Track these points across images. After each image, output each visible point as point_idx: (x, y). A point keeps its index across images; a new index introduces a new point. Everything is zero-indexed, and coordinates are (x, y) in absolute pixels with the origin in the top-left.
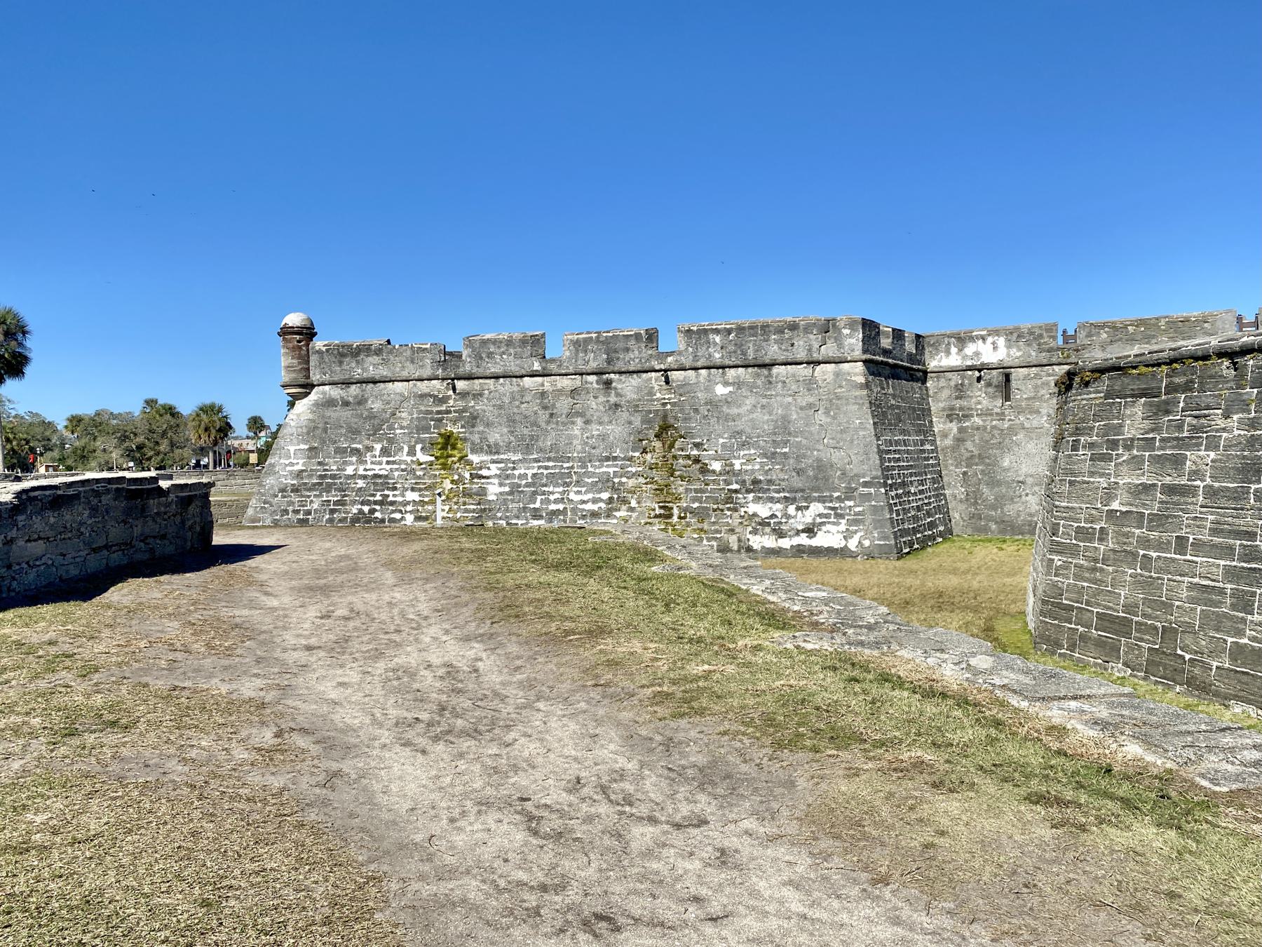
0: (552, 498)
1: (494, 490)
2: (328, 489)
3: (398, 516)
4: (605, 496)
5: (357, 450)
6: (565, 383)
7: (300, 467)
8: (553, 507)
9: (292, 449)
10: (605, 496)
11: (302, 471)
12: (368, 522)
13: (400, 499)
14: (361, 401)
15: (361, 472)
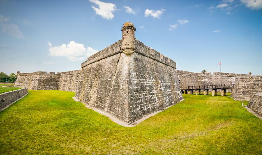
0: (168, 91)
1: (163, 89)
2: (143, 90)
3: (155, 98)
4: (171, 90)
5: (144, 76)
6: (163, 65)
7: (136, 82)
8: (168, 93)
9: (133, 74)
10: (171, 90)
11: (137, 83)
12: (152, 101)
13: (154, 93)
14: (142, 61)
15: (147, 84)
